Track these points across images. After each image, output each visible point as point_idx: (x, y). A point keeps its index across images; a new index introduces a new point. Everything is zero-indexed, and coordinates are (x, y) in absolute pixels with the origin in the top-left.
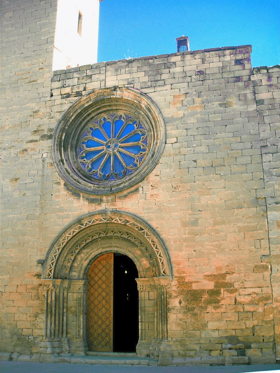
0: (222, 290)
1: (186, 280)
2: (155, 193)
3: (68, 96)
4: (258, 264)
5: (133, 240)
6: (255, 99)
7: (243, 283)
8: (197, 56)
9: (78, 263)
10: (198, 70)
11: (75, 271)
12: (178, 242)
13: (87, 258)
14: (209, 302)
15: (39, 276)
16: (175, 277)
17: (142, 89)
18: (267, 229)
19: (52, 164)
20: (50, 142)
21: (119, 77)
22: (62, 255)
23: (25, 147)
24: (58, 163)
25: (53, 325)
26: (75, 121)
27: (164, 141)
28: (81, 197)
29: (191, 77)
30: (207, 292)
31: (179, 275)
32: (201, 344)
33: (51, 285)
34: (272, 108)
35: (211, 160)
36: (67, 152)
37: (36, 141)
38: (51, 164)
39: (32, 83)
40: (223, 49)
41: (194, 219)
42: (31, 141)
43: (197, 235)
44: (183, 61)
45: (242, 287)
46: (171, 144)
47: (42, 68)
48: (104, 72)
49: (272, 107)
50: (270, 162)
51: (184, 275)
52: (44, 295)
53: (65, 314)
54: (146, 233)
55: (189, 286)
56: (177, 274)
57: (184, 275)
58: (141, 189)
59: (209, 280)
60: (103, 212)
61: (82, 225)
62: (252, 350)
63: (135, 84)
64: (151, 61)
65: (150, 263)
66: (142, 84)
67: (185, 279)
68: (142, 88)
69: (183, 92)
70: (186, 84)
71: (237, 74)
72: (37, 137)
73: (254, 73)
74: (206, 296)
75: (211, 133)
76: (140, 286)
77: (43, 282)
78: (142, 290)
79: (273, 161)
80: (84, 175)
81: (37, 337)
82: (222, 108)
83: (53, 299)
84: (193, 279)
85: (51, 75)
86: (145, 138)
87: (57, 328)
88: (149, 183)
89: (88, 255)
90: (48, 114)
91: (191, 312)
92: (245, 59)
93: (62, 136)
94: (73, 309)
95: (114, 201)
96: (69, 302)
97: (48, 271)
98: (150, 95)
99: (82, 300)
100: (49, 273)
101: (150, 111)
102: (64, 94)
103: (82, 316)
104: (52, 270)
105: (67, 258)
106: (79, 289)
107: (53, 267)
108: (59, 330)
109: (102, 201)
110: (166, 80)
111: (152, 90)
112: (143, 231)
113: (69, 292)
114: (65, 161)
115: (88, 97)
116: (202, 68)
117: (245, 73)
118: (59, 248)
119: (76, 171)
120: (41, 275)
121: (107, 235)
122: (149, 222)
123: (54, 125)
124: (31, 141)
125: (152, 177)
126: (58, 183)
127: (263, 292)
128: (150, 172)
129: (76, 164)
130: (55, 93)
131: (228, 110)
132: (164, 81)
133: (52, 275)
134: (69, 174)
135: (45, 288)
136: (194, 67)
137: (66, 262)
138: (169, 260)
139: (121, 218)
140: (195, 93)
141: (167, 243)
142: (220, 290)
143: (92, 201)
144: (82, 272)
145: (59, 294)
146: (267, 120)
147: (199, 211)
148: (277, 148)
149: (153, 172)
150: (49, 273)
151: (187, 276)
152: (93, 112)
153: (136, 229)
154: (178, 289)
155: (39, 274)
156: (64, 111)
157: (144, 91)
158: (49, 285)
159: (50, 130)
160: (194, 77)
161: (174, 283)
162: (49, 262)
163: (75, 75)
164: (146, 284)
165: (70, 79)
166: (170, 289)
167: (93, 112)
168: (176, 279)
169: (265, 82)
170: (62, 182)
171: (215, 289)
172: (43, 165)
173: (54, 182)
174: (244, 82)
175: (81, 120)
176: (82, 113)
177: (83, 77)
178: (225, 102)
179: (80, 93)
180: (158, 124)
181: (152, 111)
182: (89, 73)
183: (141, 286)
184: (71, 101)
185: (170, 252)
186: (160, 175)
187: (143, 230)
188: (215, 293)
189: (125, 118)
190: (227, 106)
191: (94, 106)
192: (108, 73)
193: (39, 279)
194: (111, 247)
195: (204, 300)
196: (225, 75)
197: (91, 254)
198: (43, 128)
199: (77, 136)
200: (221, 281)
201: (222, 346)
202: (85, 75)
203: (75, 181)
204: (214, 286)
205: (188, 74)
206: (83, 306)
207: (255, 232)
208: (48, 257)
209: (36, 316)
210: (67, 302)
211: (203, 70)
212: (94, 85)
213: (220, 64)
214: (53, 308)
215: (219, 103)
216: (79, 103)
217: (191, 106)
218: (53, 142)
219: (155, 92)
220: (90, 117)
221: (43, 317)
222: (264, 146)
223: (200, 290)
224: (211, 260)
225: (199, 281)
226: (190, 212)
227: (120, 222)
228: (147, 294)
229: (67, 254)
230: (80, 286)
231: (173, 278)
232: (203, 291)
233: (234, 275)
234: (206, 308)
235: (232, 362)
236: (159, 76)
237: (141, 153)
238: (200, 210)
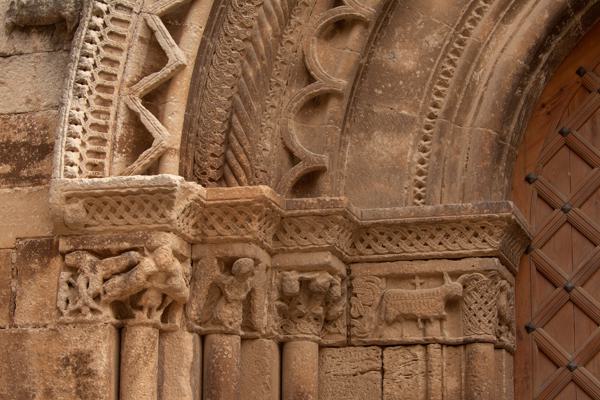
9: (433, 40)
11: (400, 125)
33: (169, 243)
77: (75, 211)
97: (127, 97)
100: (134, 120)
106: (452, 303)
107: (182, 53)
120: (46, 150)
133: (168, 132)
135: (93, 279)
150: (134, 120)
155: (20, 138)
193: (26, 190)
230: (454, 275)
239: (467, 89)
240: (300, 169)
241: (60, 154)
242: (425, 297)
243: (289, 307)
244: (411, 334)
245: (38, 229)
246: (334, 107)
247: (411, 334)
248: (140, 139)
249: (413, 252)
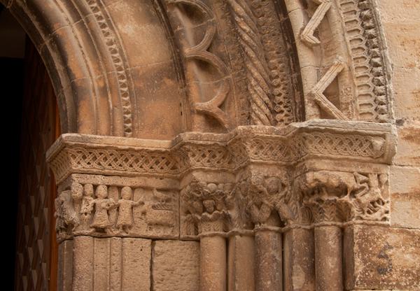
16: (409, 138)
76: (89, 189)
164: (137, 182)
166: (377, 215)
183: (102, 190)
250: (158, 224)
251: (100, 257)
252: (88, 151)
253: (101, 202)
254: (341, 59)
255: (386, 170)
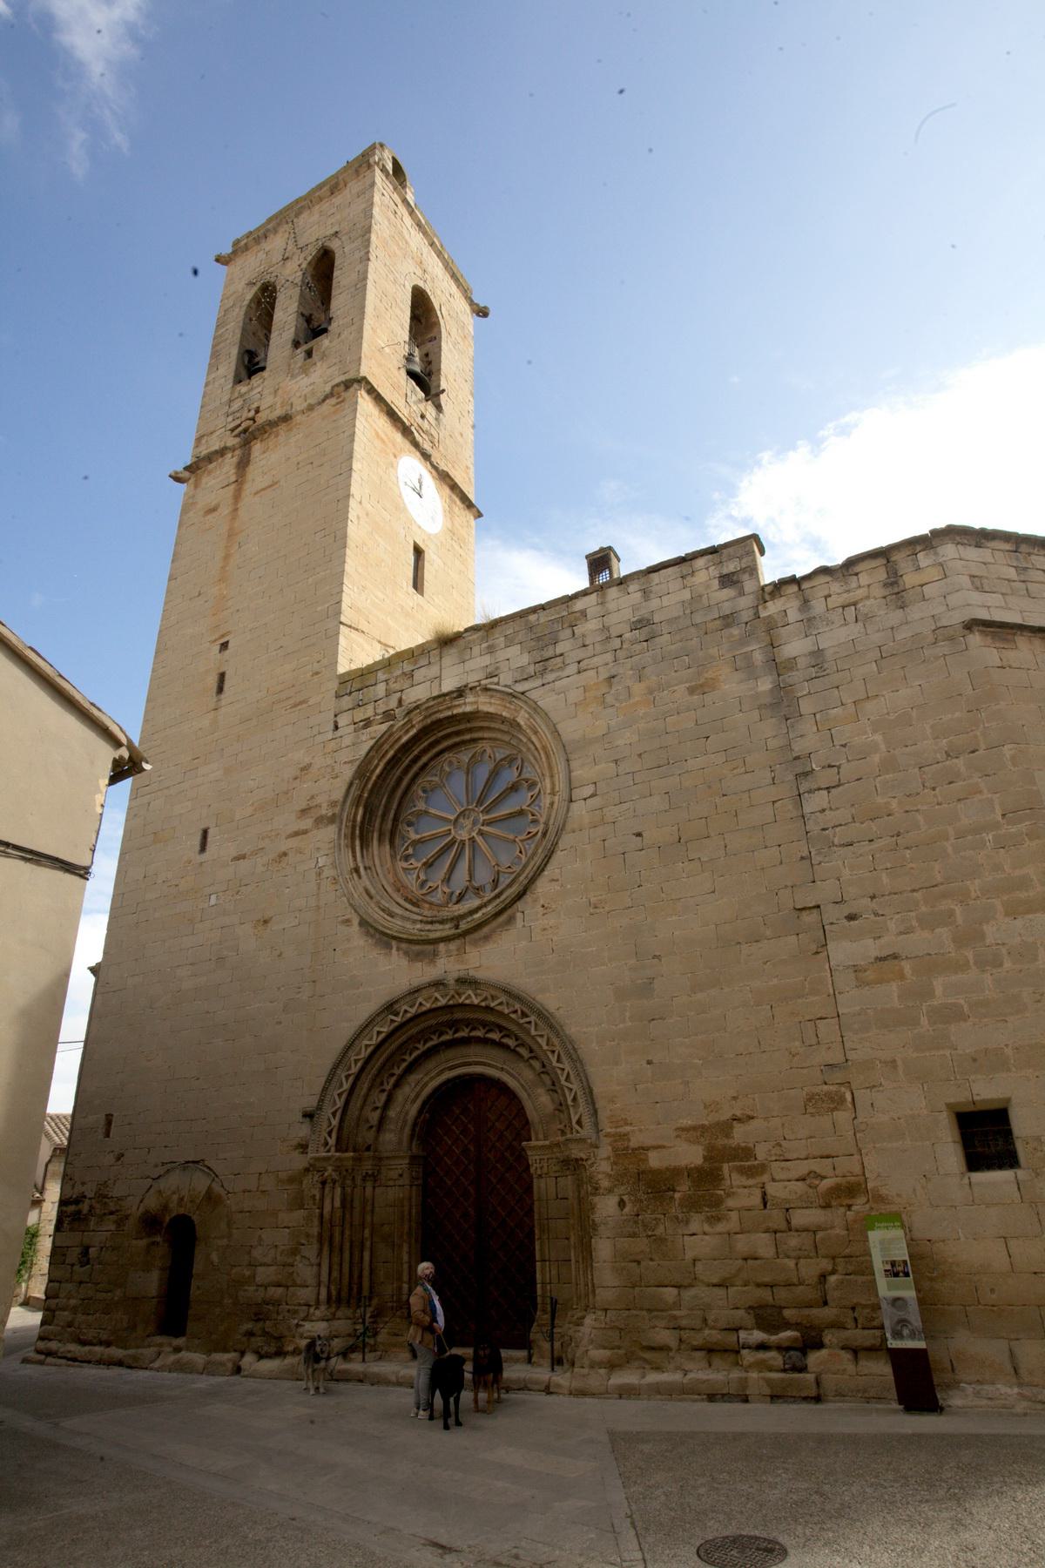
0: (726, 1167)
1: (633, 1143)
2: (552, 922)
3: (368, 723)
4: (817, 1090)
5: (511, 1042)
6: (774, 660)
7: (781, 1146)
8: (633, 587)
9: (398, 1110)
10: (635, 619)
12: (608, 1043)
13: (417, 1096)
14: (692, 1205)
15: (303, 1147)
16: (605, 1136)
17: (517, 684)
18: (832, 992)
19: (335, 880)
20: (331, 832)
21: (470, 665)
22: (357, 1091)
23: (285, 845)
24: (347, 877)
25: (335, 1274)
26: (384, 780)
27: (565, 795)
28: (394, 949)
29: (621, 636)
30: (686, 1174)
31: (613, 1130)
32: (680, 1328)
33: (330, 1169)
34: (818, 675)
35: (675, 828)
36: (370, 850)
37: (305, 832)
38: (335, 879)
39: (299, 707)
40: (690, 557)
41: (645, 980)
42: (296, 834)
43: (653, 1020)
44: (602, 604)
45: (778, 1158)
46: (583, 801)
47: (317, 673)
48: (438, 659)
49: (816, 672)
50: (824, 810)
51: (628, 1128)
52: (314, 1196)
53: (368, 1244)
54: (533, 1024)
55: (641, 1160)
56: (611, 1128)
57: (628, 1128)
58: (519, 915)
59: (688, 1141)
60: (438, 984)
61: (397, 1014)
62: (824, 1352)
63: (501, 676)
64: (532, 618)
65: (553, 1100)
66: (515, 674)
67: (629, 1140)
68: (516, 682)
69: (604, 674)
70: (609, 657)
71: (727, 609)
72: (307, 823)
73: (767, 597)
74: (684, 1188)
75: (672, 762)
78: (539, 1172)
79: (831, 809)
80: (406, 899)
81: (296, 1308)
82: (696, 697)
83: (338, 1204)
84: (649, 1142)
85: (333, 686)
86: (536, 797)
87: (346, 1281)
88: (535, 901)
89: (418, 1088)
90: (329, 770)
91: (650, 1233)
92: (743, 570)
93: (356, 814)
94: (386, 1229)
95: (462, 951)
96: (377, 1209)
98: (533, 695)
99: (406, 1203)
101: (536, 733)
102: (361, 721)
103: (405, 1248)
104: (332, 1130)
105: (371, 1099)
106: (401, 1175)
107: (335, 1122)
108: (350, 1289)
109: (437, 955)
110: (565, 655)
111: (539, 682)
112: (527, 1020)
113: (378, 1183)
114: (362, 870)
115: (406, 720)
116: (643, 612)
117: (746, 602)
118: (349, 1075)
119: (389, 890)
121: (456, 1035)
122: (540, 998)
123: (338, 795)
124: (296, 834)
125: (543, 887)
126: (347, 922)
127: (837, 1173)
128: (539, 874)
129: (391, 876)
130: (342, 721)
131: (708, 698)
132: (562, 657)
133: (332, 1141)
134: (371, 898)
136: (628, 615)
137: (368, 1108)
138: (589, 1092)
139: (479, 991)
140: (631, 672)
141: (582, 1046)
142: (720, 1169)
143: (416, 957)
144: (407, 1130)
145: (352, 1191)
146: (806, 707)
147: (655, 957)
148: (839, 773)
149: (546, 873)
151: (633, 1131)
152: (425, 751)
153: (513, 1016)
154: (615, 1167)
156: (357, 759)
157: (520, 688)
158: (325, 1170)
159: (333, 804)
160: (627, 635)
161: (605, 1151)
162: (328, 1111)
163: (381, 676)
165: (372, 686)
167: (425, 751)
168: (608, 1140)
169: (793, 615)
170: (356, 921)
171: (707, 1165)
172: (319, 884)
173: (340, 919)
174: (744, 625)
175: (398, 773)
176: (400, 759)
177: (397, 677)
178: (702, 680)
179: (390, 714)
180: (554, 760)
181: (539, 730)
182: (407, 667)
183: (538, 1161)
184: (373, 735)
185: (590, 1070)
186: (559, 877)
187: (527, 1016)
188: (707, 1175)
189: (492, 756)
190: (706, 690)
191: (423, 740)
192: (447, 661)
194: (469, 1064)
195: (680, 1199)
196: (698, 618)
197: (426, 1085)
198: (318, 800)
199: (393, 812)
200: (721, 1142)
201: (738, 1337)
202: (399, 672)
203: (382, 913)
204: (705, 1158)
205: (614, 633)
206: (410, 1221)
207: (800, 1001)
208: (323, 1100)
209: (294, 1252)
210: (372, 1211)
211: (646, 615)
212: (418, 693)
213: (686, 595)
214: (337, 1231)
215: (687, 685)
216: (390, 736)
217: (624, 704)
218: (337, 829)
219: (543, 685)
220: (420, 763)
221: (310, 1251)
222: (806, 774)
223: (667, 1169)
224: (690, 1085)
225: (665, 1144)
226: (632, 962)
227: (476, 1001)
228: (551, 1182)
229: (369, 1090)
231: (602, 1138)
232: (676, 1172)
233: (754, 1123)
234: (687, 1222)
235: (768, 1391)
236: (551, 647)
237: (529, 833)
238: (658, 954)
239: (405, 1122)
240: (366, 1145)
241: (310, 1148)
242: (394, 1174)
243: (364, 1180)
244: (391, 1183)
245: (307, 1165)
246: (374, 1129)
247: (391, 1183)
248: (326, 1144)
249: (392, 1163)
250: (556, 1172)
251: (543, 1185)
252: (534, 1148)
253: (538, 1165)
254: (581, 1109)
255: (595, 1150)
